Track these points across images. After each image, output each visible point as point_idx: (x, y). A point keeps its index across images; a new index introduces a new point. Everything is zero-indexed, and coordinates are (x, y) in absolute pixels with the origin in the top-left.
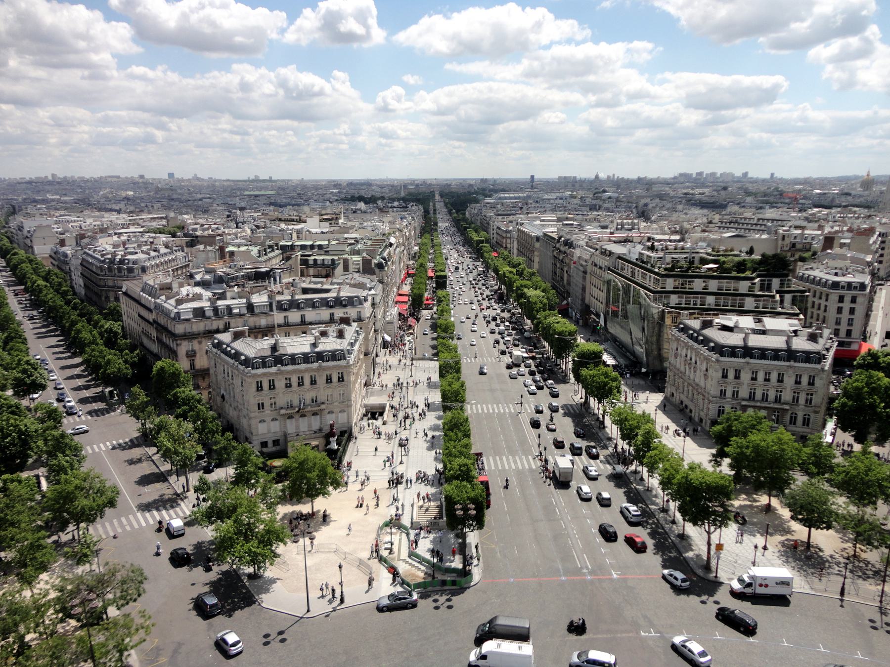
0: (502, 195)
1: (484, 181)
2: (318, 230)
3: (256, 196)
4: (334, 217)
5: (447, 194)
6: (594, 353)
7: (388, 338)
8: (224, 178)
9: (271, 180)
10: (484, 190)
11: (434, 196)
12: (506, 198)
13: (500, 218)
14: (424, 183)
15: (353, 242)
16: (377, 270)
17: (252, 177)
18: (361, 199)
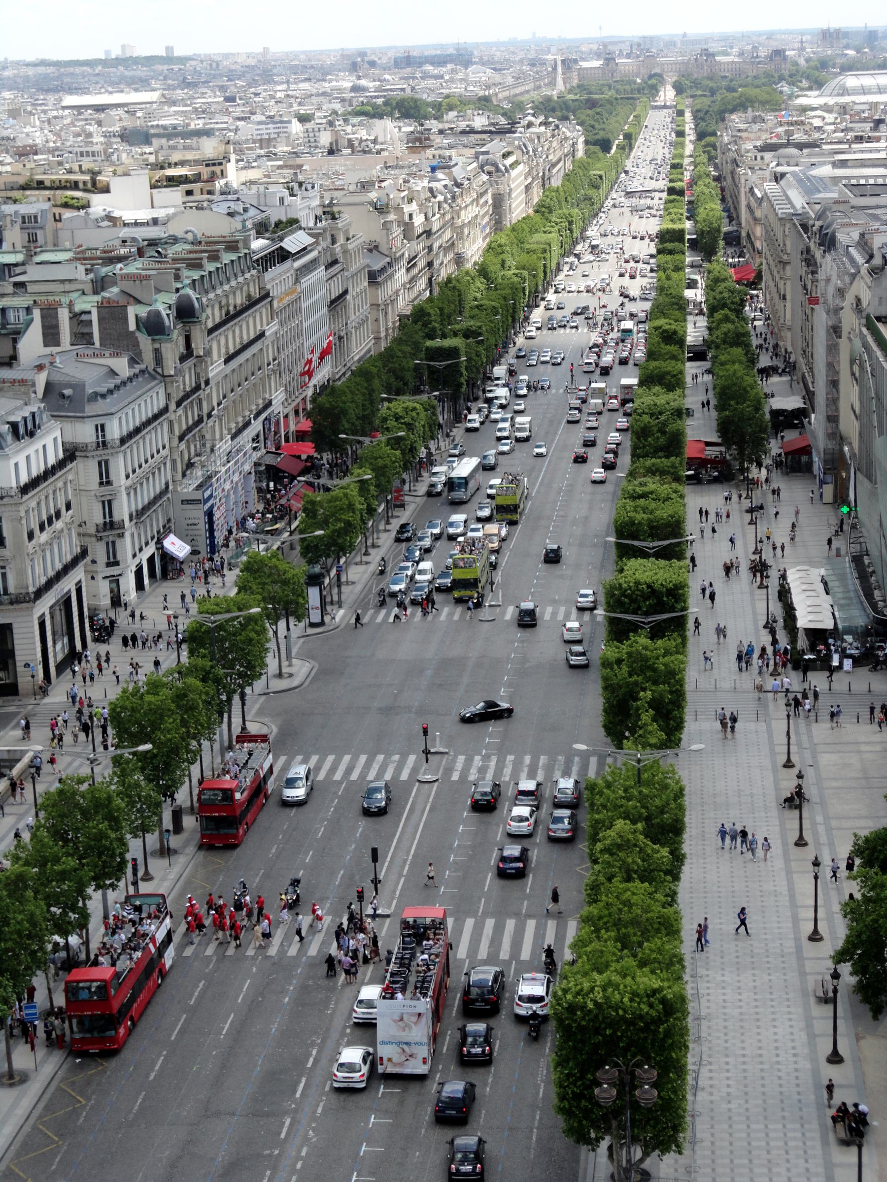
0: (851, 81)
1: (829, 36)
2: (144, 215)
3: (100, 108)
4: (205, 172)
5: (696, 84)
6: (652, 591)
7: (177, 547)
8: (31, 58)
9: (169, 59)
10: (824, 64)
11: (652, 89)
12: (864, 91)
13: (768, 156)
14: (643, 49)
15: (123, 251)
16: (145, 342)
17: (116, 53)
18: (406, 109)
